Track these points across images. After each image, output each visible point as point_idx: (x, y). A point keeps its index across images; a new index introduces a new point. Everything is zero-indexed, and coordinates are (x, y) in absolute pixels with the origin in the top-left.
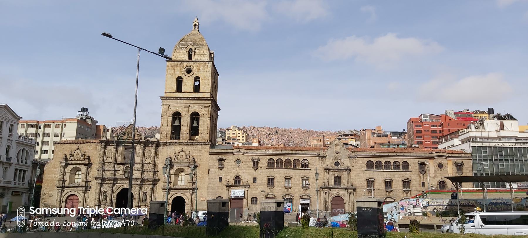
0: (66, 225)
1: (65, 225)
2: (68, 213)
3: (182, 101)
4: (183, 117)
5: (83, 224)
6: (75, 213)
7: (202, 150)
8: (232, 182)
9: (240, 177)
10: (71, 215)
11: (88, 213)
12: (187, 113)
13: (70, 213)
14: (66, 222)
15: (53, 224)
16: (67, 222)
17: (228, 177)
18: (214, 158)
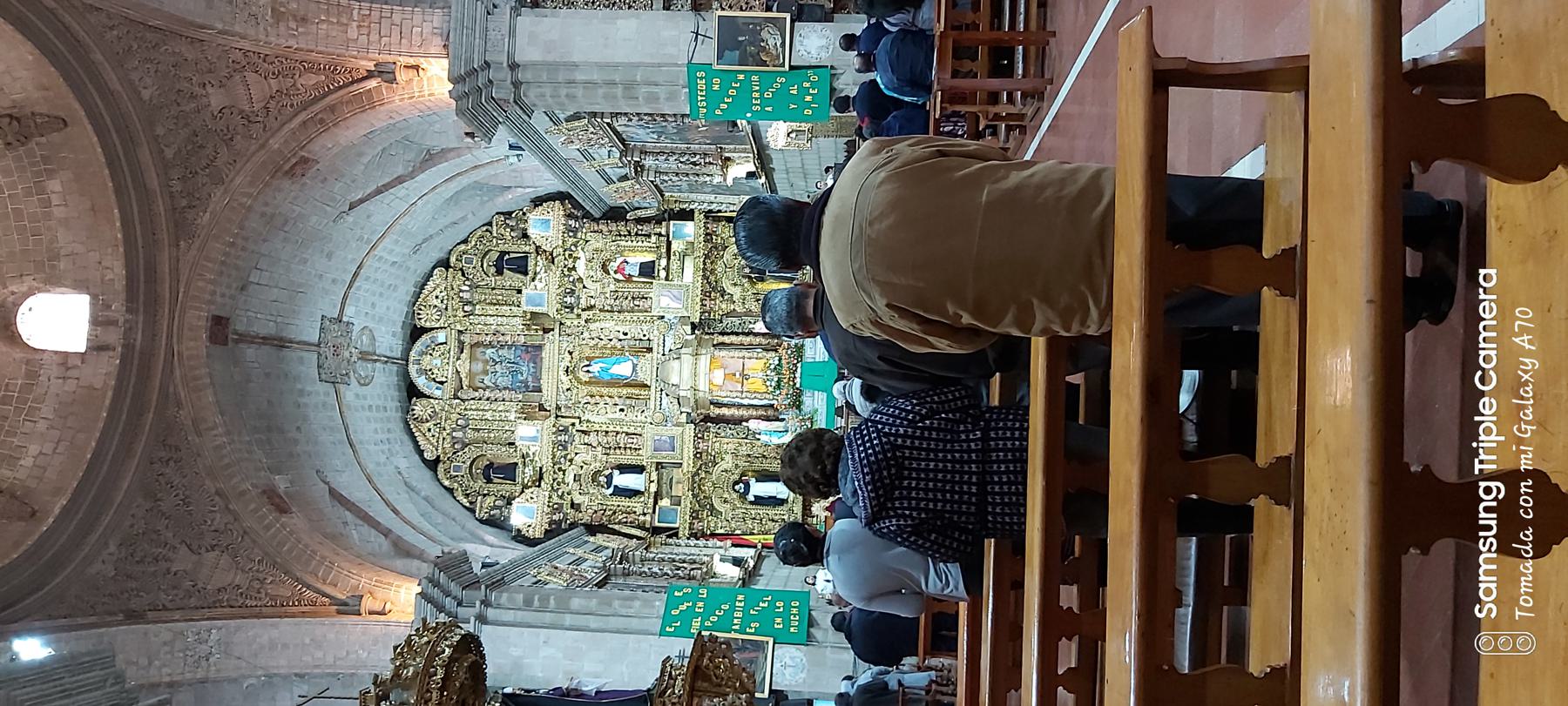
0: (1530, 510)
1: (1529, 514)
2: (1494, 504)
5: (1525, 458)
6: (1492, 484)
10: (1501, 497)
11: (1495, 445)
13: (1496, 499)
14: (1521, 511)
15: (1527, 548)
16: (1523, 507)
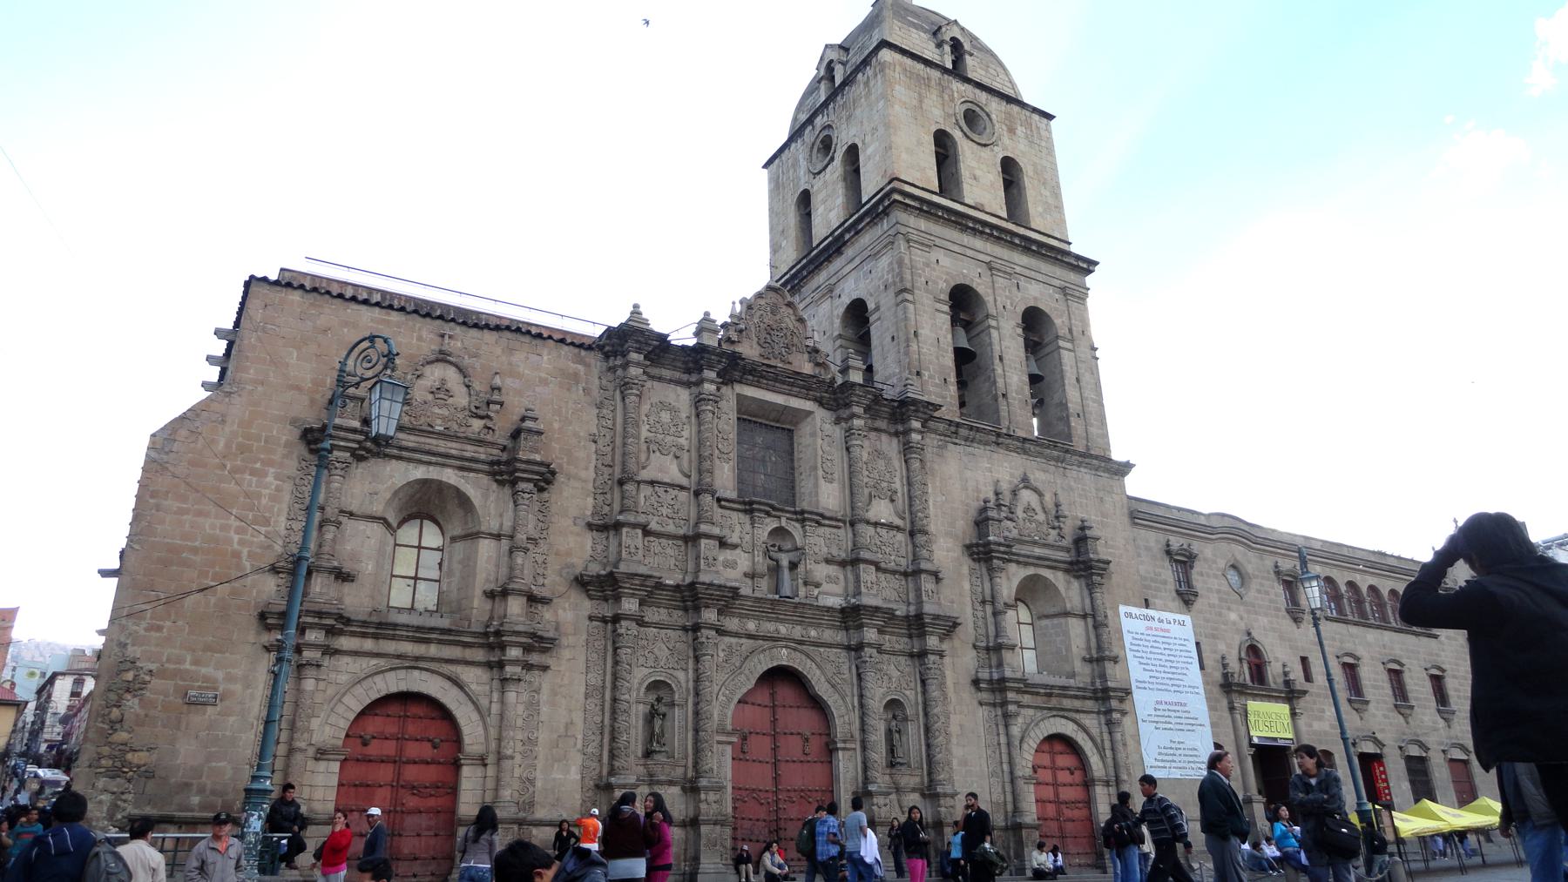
3: (978, 243)
4: (994, 318)
7: (1101, 494)
8: (1242, 673)
9: (1259, 646)
12: (1008, 307)
17: (1222, 647)
18: (1152, 544)
